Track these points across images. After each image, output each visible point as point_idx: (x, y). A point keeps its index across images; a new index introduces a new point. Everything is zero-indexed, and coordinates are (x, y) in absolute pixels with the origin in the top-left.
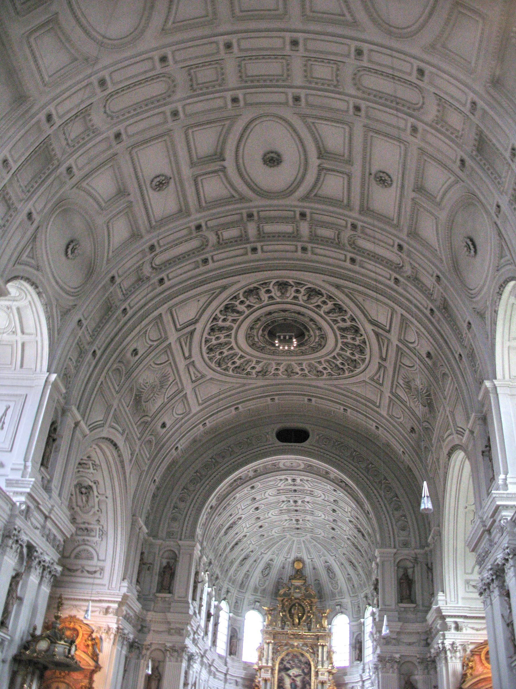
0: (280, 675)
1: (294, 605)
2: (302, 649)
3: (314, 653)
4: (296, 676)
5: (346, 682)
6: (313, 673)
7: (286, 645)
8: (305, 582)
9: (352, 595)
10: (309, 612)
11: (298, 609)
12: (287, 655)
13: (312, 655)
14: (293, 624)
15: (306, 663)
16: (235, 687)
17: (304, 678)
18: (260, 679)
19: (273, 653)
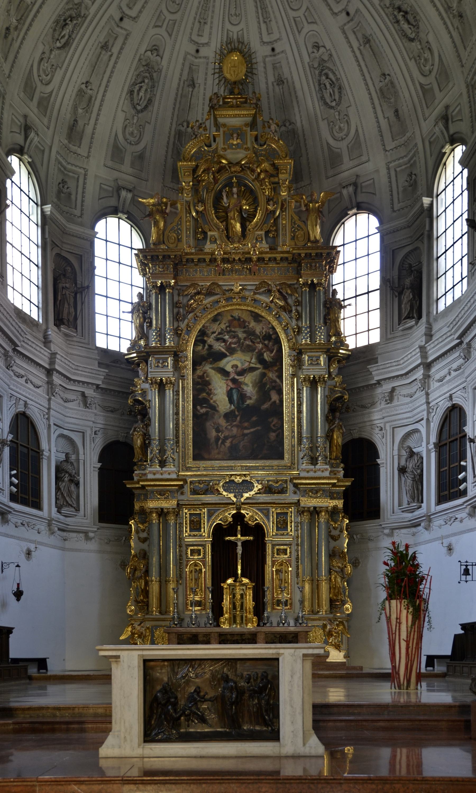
0: (199, 372)
1: (229, 184)
2: (255, 300)
3: (286, 309)
4: (242, 373)
5: (376, 378)
6: (286, 361)
7: (209, 293)
8: (255, 116)
9: (390, 145)
10: (269, 200)
11: (238, 196)
12: (215, 319)
13: (284, 313)
14: (228, 237)
15: (267, 337)
16: (82, 408)
17: (263, 375)
18: (146, 386)
19: (176, 318)
